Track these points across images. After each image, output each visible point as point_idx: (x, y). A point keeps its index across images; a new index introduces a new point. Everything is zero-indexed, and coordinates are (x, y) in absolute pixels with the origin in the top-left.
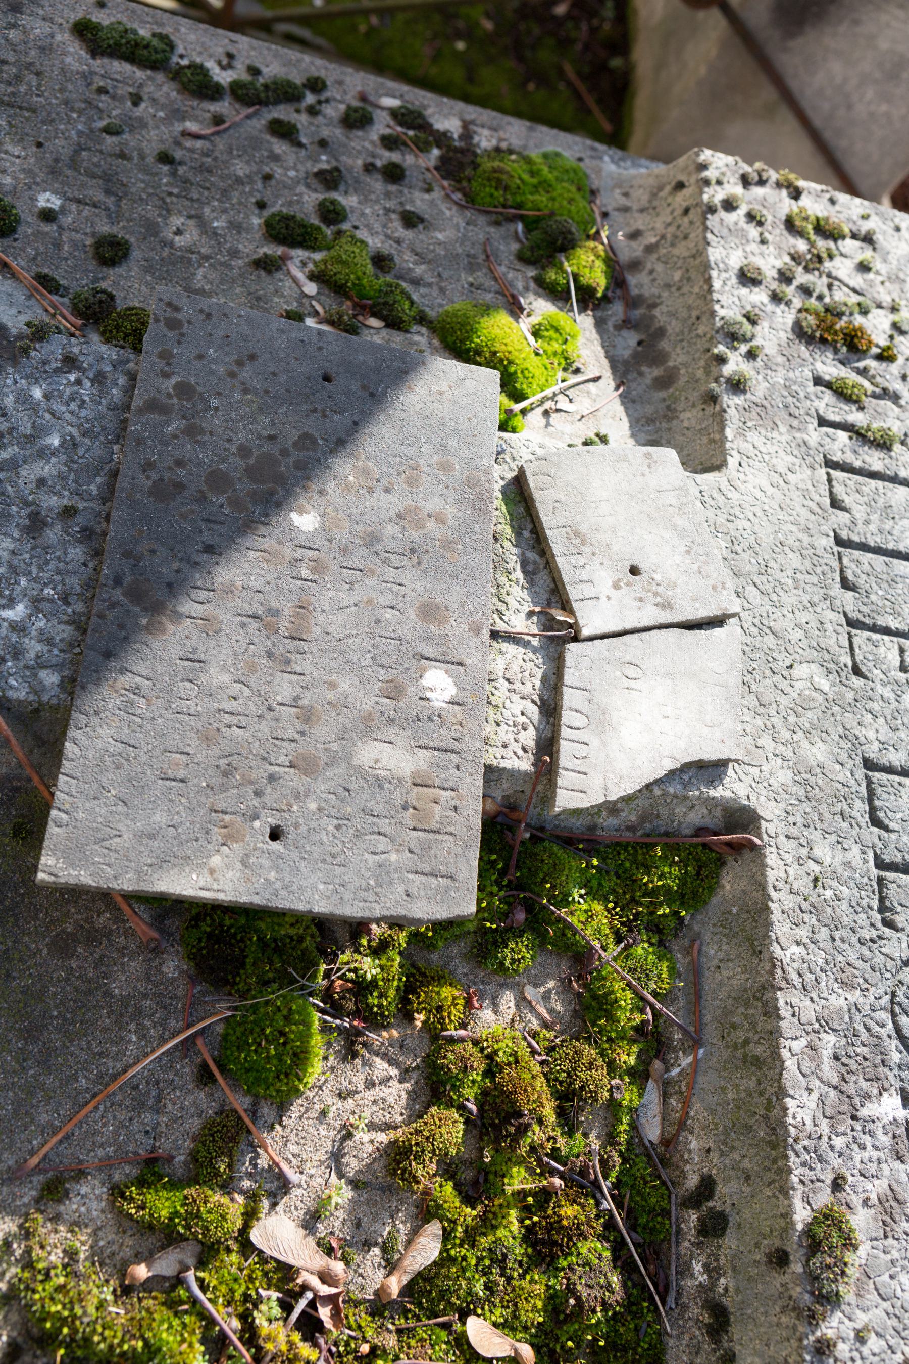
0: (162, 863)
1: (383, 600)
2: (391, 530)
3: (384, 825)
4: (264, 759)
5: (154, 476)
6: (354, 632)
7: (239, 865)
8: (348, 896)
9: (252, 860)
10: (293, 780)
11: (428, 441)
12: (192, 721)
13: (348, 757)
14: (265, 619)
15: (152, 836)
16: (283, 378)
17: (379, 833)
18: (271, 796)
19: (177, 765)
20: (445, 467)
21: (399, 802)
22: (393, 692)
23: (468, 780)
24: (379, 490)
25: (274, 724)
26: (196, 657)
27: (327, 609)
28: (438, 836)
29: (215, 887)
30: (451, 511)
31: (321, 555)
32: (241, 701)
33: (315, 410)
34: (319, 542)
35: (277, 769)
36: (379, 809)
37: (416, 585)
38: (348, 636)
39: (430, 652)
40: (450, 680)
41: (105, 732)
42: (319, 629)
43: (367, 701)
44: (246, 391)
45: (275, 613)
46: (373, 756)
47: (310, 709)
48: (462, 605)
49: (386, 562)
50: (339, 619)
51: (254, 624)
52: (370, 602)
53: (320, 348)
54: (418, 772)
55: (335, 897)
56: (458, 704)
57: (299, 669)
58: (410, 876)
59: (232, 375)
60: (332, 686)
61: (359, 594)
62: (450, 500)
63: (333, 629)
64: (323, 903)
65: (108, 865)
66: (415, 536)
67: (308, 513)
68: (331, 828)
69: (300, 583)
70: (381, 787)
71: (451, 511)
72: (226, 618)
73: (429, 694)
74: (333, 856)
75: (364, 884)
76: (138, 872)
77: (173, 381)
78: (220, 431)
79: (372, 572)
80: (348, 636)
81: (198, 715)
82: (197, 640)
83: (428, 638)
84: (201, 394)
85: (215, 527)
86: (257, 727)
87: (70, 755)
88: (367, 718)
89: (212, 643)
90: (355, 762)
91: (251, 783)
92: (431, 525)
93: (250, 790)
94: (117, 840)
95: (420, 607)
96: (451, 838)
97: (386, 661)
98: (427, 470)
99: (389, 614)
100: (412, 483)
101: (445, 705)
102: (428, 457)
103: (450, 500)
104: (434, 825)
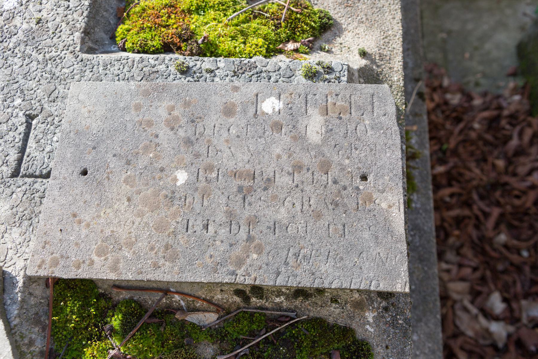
0: (390, 231)
1: (225, 135)
2: (181, 133)
3: (351, 128)
4: (325, 187)
5: (162, 261)
6: (246, 148)
7: (385, 194)
8: (390, 142)
9: (380, 188)
10: (334, 172)
11: (122, 116)
12: (310, 225)
13: (318, 146)
14: (244, 193)
15: (377, 238)
16: (88, 197)
17: (356, 129)
18: (345, 182)
19: (336, 229)
20: (138, 107)
21: (338, 121)
22: (278, 127)
23: (320, 90)
24: (157, 140)
25: (305, 184)
26: (273, 227)
27: (234, 162)
28: (353, 103)
29: (397, 204)
30: (166, 104)
31: (202, 167)
32: (295, 201)
33: (108, 178)
34: (194, 169)
35: (330, 180)
36: (343, 130)
37: (214, 119)
38: (249, 151)
39: (252, 111)
40: (267, 100)
41: (323, 269)
42: (247, 165)
43: (284, 139)
44: (99, 216)
45: (240, 189)
46: (315, 134)
47: (294, 166)
48: (222, 96)
49: (201, 134)
50: (239, 155)
51: (249, 199)
52: (227, 141)
53: (65, 178)
54: (320, 113)
55: (392, 148)
56: (280, 96)
57: (272, 174)
58: (375, 114)
59: (88, 225)
60: (279, 157)
61: (223, 147)
62: (159, 104)
63: (246, 158)
64: (396, 153)
65: (396, 257)
66: (183, 121)
67: (176, 176)
68: (357, 152)
69: (220, 177)
70: (331, 130)
71: (166, 104)
72: (247, 213)
73: (277, 110)
74: (371, 150)
75: (383, 135)
76: (397, 242)
77: (95, 258)
78: (127, 228)
79: (209, 141)
80: (249, 151)
81: (306, 222)
82: (263, 227)
83: (245, 111)
84: (103, 241)
85: (190, 224)
86: (308, 192)
87: (339, 284)
88: (295, 138)
89: (263, 219)
90: (320, 143)
91: (339, 192)
92: (176, 113)
93: (343, 192)
94: (381, 254)
95: (227, 116)
96: (353, 97)
97: (261, 131)
98: (141, 117)
99: (233, 131)
100: (150, 123)
101: (281, 103)
102: (132, 116)
103: (159, 104)
104: (347, 105)
